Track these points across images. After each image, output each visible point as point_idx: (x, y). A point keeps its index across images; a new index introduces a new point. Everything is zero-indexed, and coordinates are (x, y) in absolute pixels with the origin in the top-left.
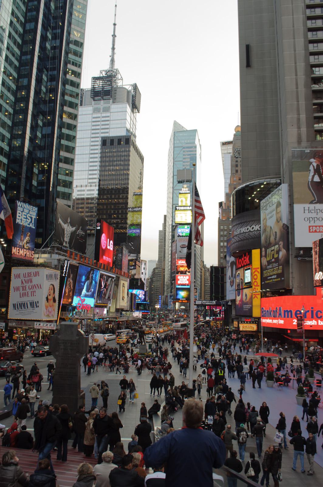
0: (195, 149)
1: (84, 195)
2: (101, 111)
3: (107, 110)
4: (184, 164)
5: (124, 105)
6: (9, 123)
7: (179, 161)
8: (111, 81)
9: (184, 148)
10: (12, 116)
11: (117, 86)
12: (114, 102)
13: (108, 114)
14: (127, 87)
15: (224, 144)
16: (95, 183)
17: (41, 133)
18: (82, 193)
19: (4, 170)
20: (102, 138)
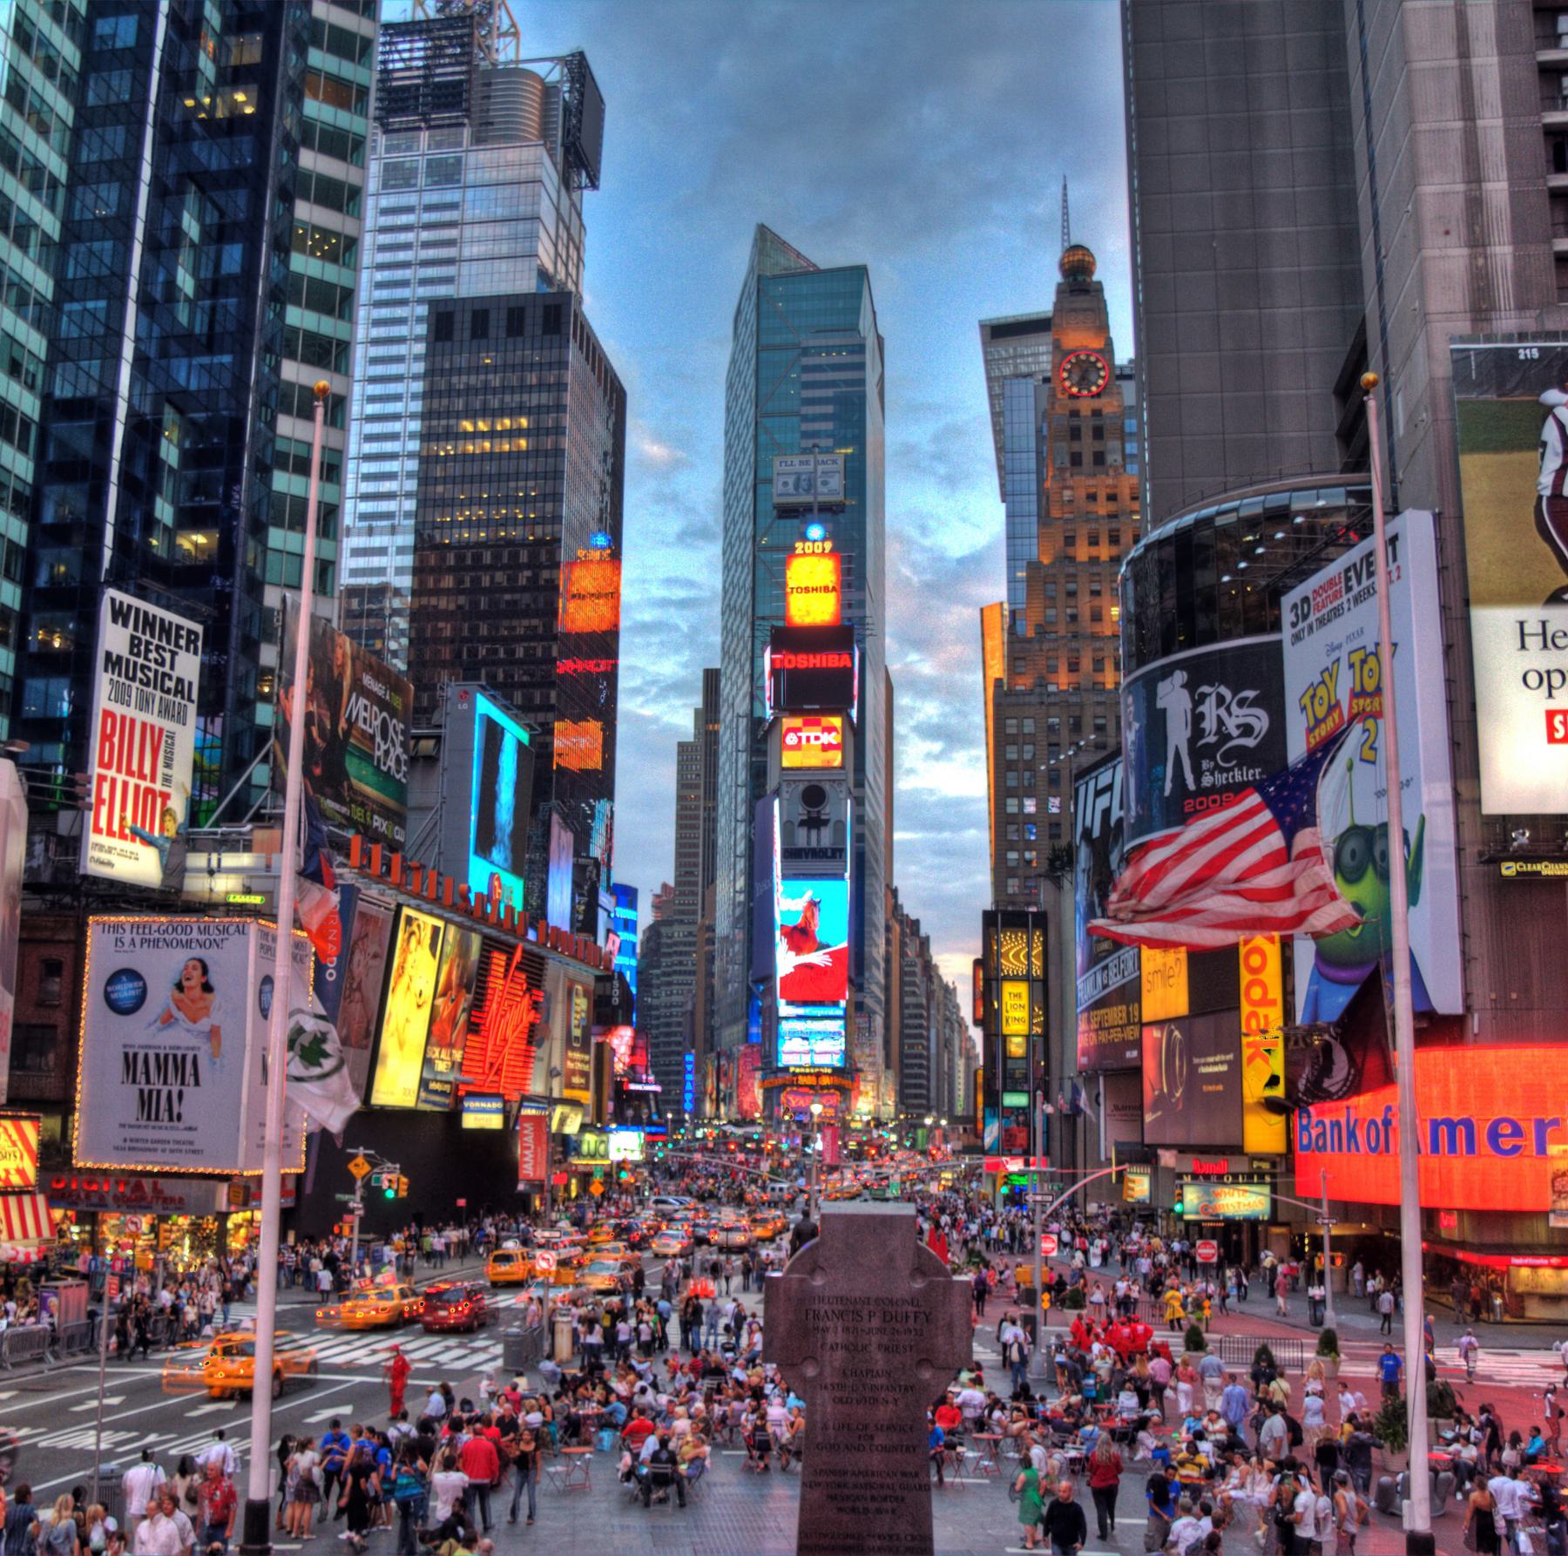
0: (856, 359)
1: (381, 571)
2: (422, 180)
3: (446, 173)
4: (804, 427)
5: (527, 154)
6: (50, 223)
7: (780, 415)
8: (466, 43)
9: (805, 352)
10: (61, 194)
11: (494, 65)
12: (478, 140)
13: (451, 196)
14: (541, 69)
15: (998, 332)
16: (389, 515)
17: (195, 273)
18: (376, 561)
19: (23, 448)
20: (433, 303)
